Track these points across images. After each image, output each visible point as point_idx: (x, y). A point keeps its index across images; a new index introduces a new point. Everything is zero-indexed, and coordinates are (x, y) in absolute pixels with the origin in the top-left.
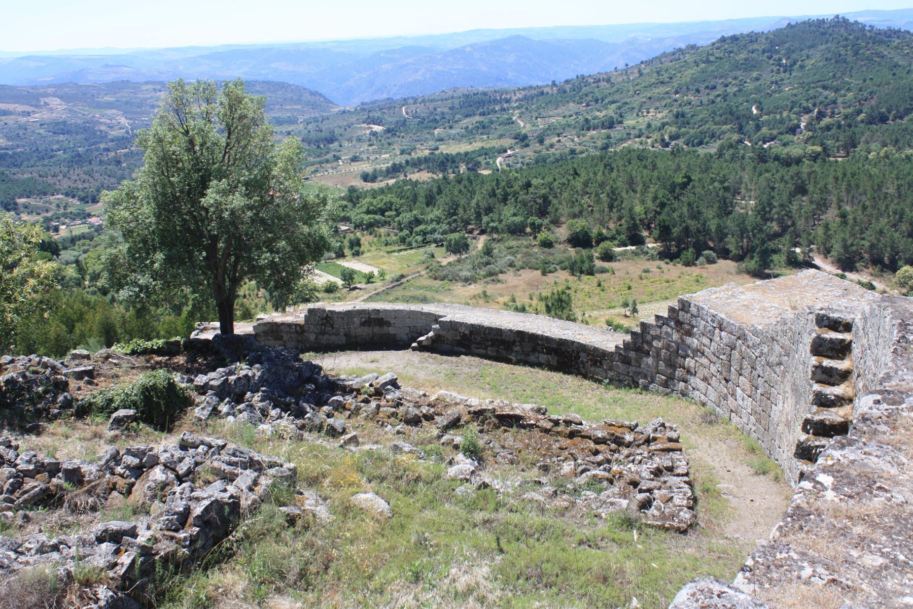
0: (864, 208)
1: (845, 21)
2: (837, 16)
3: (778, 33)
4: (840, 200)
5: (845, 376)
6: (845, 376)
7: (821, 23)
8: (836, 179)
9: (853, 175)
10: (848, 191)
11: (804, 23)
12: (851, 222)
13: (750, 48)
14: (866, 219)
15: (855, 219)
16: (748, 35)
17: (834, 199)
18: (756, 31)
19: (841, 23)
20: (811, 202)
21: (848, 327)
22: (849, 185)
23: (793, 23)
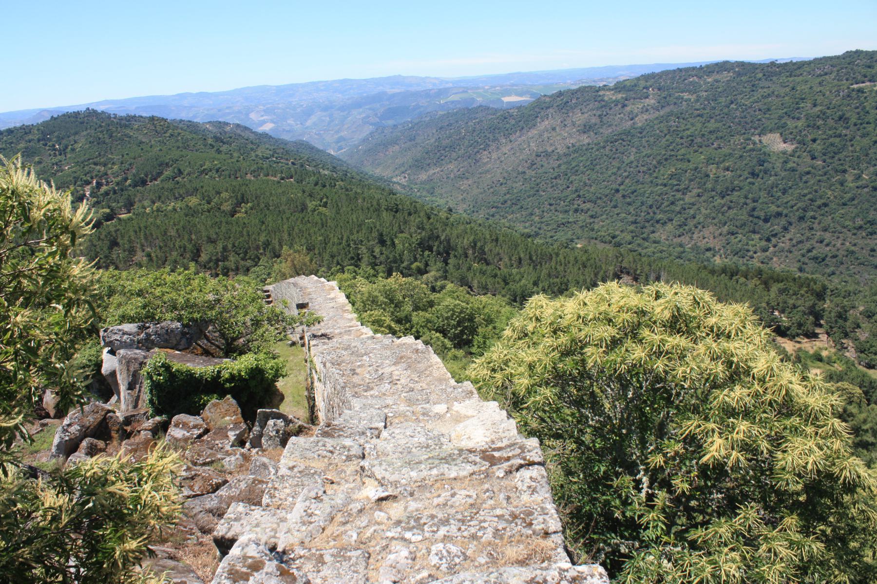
0: (161, 248)
1: (95, 111)
2: (88, 109)
3: (45, 124)
4: (143, 246)
5: (271, 302)
6: (271, 302)
7: (77, 114)
8: (136, 232)
9: (146, 227)
10: (146, 239)
11: (64, 115)
12: (155, 258)
13: (27, 139)
14: (163, 255)
15: (157, 256)
16: (21, 128)
17: (138, 246)
18: (26, 124)
19: (91, 114)
20: (124, 251)
21: (268, 291)
22: (146, 234)
23: (55, 116)
